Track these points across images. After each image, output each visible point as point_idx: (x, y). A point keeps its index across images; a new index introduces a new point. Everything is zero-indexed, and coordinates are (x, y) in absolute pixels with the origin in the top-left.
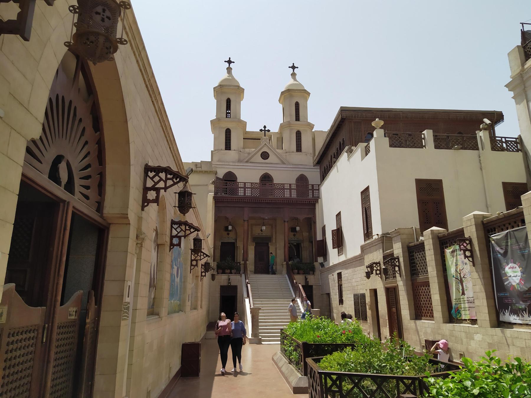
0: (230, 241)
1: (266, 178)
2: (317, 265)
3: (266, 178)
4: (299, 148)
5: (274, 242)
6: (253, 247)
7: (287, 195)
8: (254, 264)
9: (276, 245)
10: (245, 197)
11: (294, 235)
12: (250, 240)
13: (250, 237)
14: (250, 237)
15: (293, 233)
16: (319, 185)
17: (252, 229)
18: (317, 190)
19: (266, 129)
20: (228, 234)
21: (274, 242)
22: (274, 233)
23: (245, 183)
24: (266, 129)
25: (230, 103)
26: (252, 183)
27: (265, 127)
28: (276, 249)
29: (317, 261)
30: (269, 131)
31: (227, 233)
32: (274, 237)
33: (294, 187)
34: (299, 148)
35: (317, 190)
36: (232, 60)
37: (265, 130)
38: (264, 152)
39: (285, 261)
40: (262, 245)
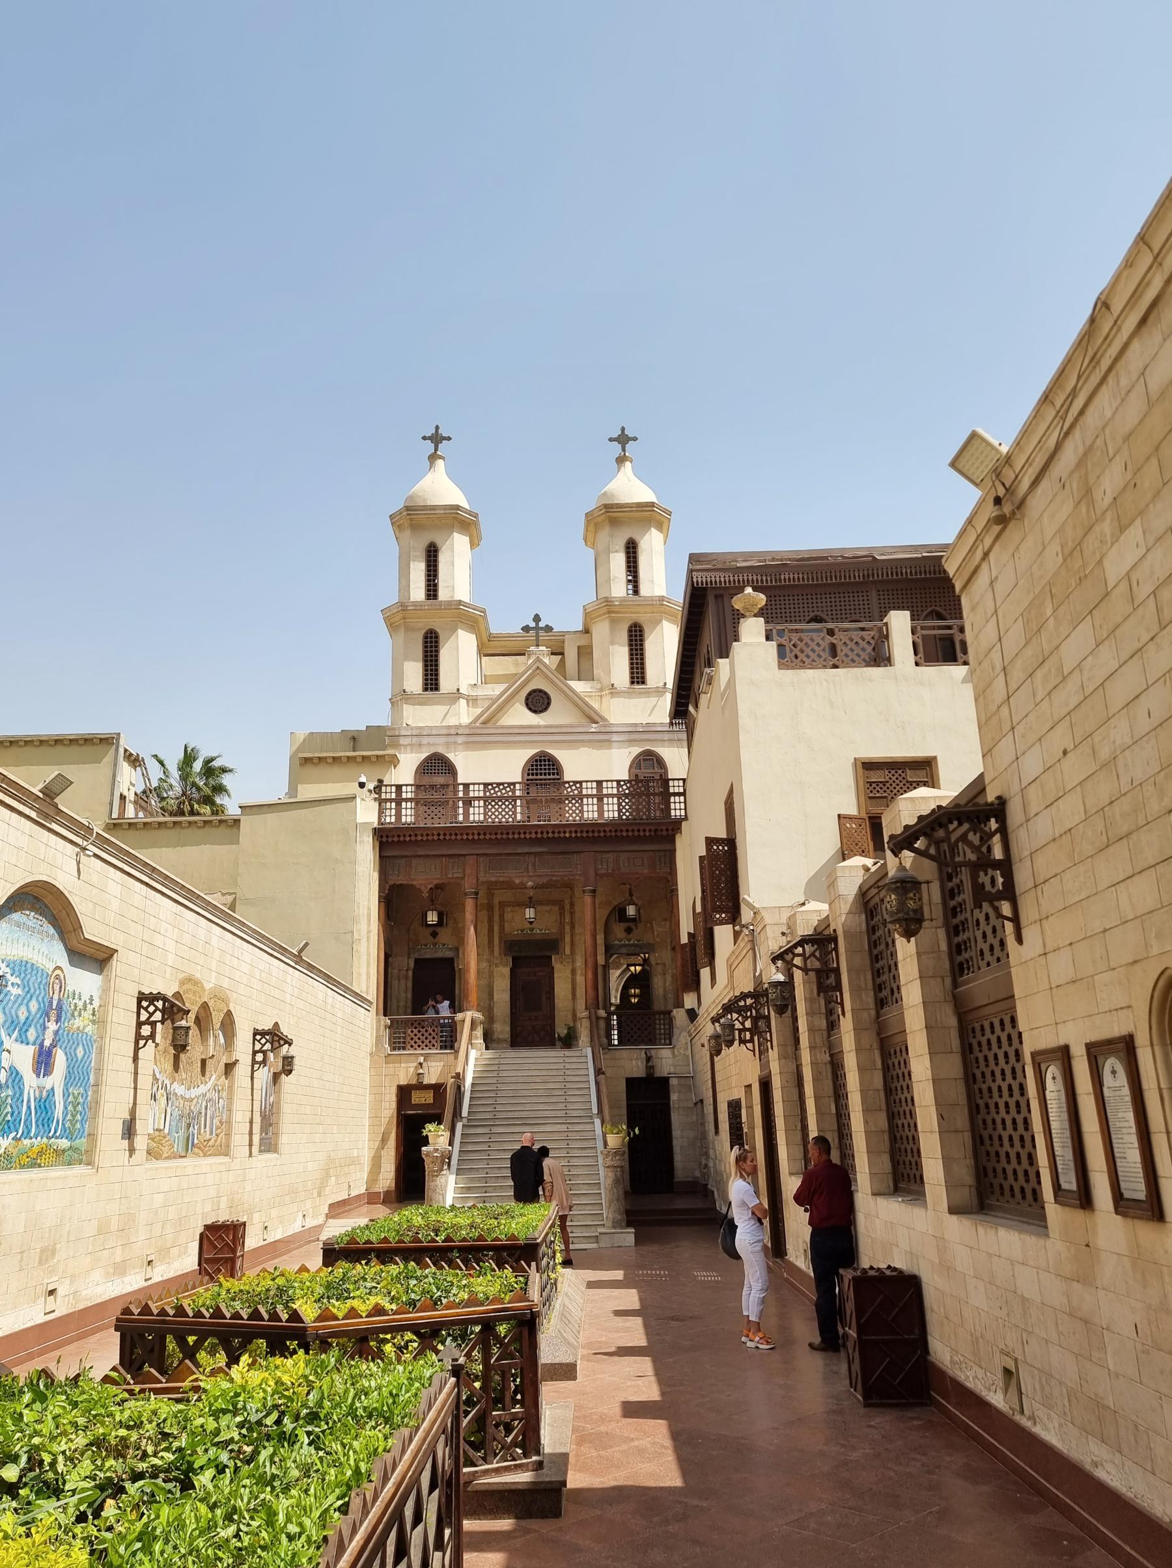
0: (440, 955)
1: (543, 769)
2: (679, 1015)
3: (543, 769)
4: (638, 674)
5: (568, 951)
6: (506, 971)
8: (508, 1019)
9: (574, 961)
11: (629, 930)
12: (496, 949)
13: (496, 941)
14: (496, 941)
15: (624, 925)
16: (684, 780)
17: (502, 916)
18: (679, 794)
19: (542, 624)
21: (568, 951)
22: (567, 928)
24: (542, 624)
26: (486, 785)
27: (537, 618)
28: (573, 972)
29: (679, 1004)
30: (548, 629)
32: (568, 939)
33: (610, 789)
34: (638, 674)
35: (679, 794)
37: (537, 628)
38: (534, 691)
40: (530, 963)
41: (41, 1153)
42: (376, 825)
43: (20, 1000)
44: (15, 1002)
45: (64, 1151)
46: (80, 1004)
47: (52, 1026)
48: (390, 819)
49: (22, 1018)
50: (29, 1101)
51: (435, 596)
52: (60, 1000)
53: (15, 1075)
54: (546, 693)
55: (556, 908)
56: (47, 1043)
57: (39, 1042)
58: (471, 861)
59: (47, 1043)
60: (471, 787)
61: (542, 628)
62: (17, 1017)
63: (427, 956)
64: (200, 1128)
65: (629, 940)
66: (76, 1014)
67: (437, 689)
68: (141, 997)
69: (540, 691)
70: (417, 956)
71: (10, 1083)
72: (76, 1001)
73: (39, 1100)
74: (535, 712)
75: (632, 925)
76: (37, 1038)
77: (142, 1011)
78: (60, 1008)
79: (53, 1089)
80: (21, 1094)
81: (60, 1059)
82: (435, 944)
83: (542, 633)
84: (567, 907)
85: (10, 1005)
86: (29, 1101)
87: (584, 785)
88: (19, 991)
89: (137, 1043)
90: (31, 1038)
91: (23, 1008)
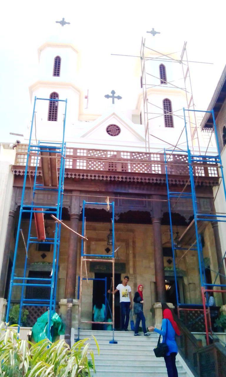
4: (169, 122)
7: (157, 169)
9: (135, 278)
10: (74, 170)
16: (216, 158)
19: (116, 95)
20: (44, 256)
22: (131, 256)
23: (75, 149)
24: (116, 95)
25: (59, 62)
27: (113, 92)
31: (41, 253)
32: (131, 264)
36: (66, 20)
37: (113, 97)
39: (157, 300)
42: (13, 164)
48: (23, 162)
51: (58, 75)
54: (117, 127)
55: (124, 244)
58: (74, 194)
60: (78, 151)
61: (116, 97)
63: (38, 270)
65: (170, 268)
67: (55, 119)
69: (115, 125)
70: (31, 270)
74: (112, 135)
75: (170, 258)
82: (43, 262)
83: (116, 99)
84: (131, 244)
87: (152, 155)
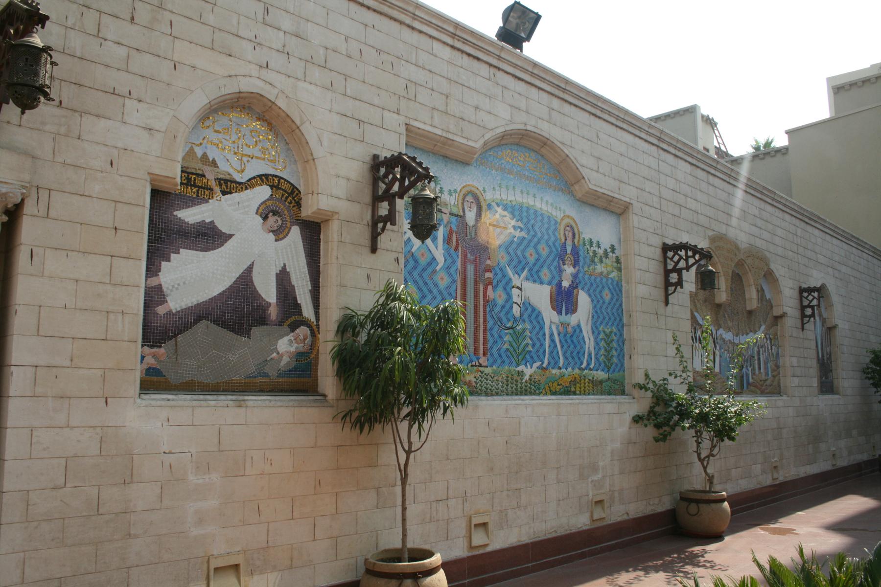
41: (574, 382)
43: (525, 243)
44: (519, 244)
45: (601, 382)
46: (600, 252)
47: (569, 270)
49: (532, 260)
50: (552, 335)
52: (574, 247)
53: (531, 312)
56: (566, 284)
57: (555, 282)
59: (566, 284)
62: (525, 257)
64: (754, 369)
66: (596, 260)
68: (666, 248)
71: (525, 316)
72: (596, 249)
73: (564, 335)
76: (553, 278)
77: (668, 261)
78: (575, 252)
79: (579, 326)
80: (542, 328)
81: (583, 299)
85: (514, 246)
86: (552, 335)
88: (523, 234)
89: (666, 290)
90: (546, 279)
91: (531, 250)
